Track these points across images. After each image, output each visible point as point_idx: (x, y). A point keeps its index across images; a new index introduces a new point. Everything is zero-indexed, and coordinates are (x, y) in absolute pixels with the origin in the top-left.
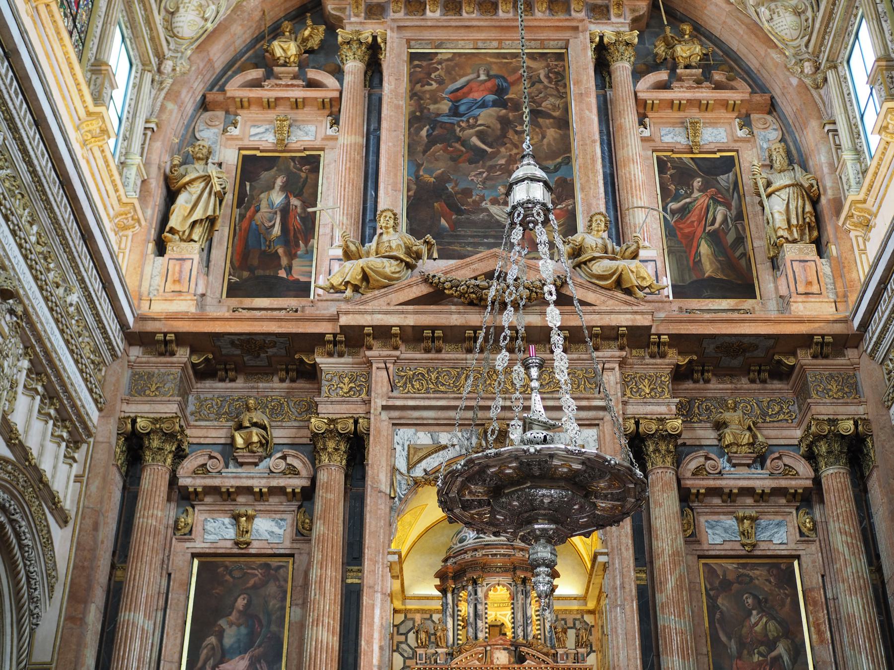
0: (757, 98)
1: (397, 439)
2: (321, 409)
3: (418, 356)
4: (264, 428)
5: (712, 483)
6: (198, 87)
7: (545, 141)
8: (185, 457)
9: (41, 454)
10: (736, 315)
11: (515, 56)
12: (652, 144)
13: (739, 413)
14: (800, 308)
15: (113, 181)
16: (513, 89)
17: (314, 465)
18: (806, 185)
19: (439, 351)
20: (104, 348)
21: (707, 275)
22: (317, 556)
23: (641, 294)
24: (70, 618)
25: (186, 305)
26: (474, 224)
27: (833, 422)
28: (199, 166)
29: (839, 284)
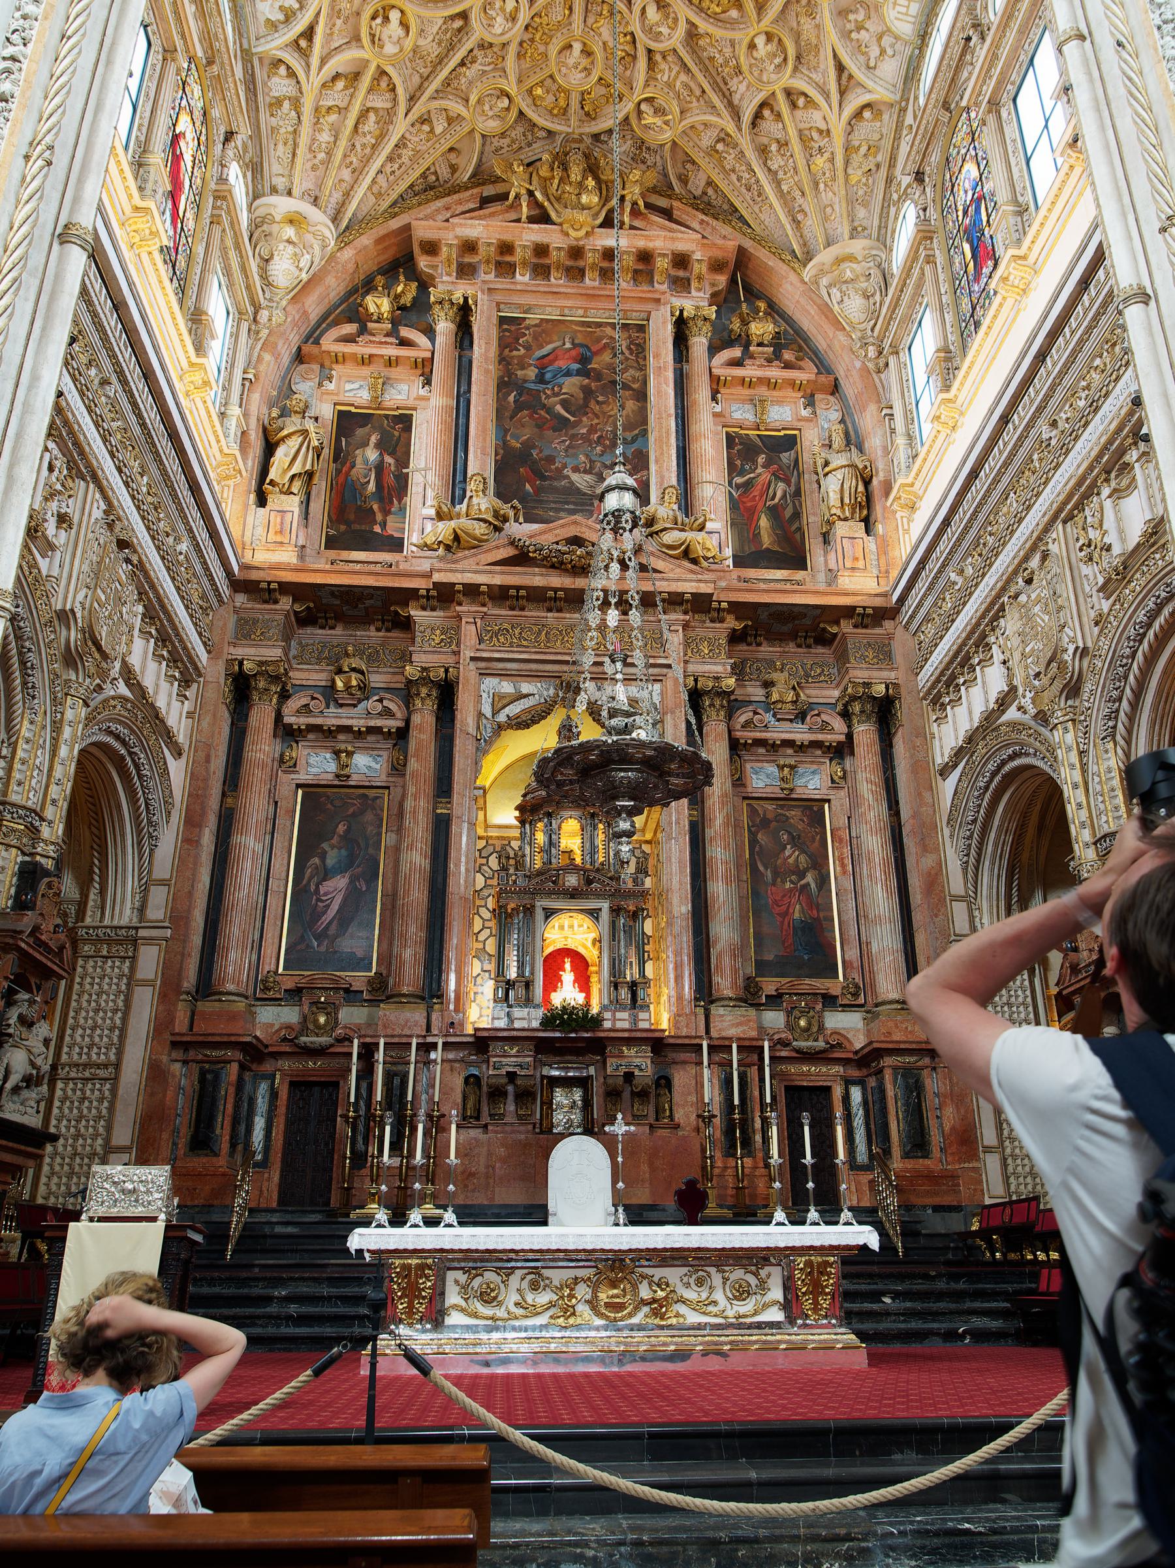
0: (823, 379)
1: (483, 687)
2: (415, 658)
3: (503, 612)
4: (362, 673)
5: (758, 735)
6: (294, 339)
8: (289, 697)
9: (156, 693)
10: (788, 586)
11: (599, 325)
13: (786, 674)
14: (846, 582)
15: (215, 432)
16: (596, 359)
17: (408, 708)
19: (522, 609)
20: (211, 595)
22: (411, 789)
23: (705, 564)
24: (186, 840)
25: (288, 556)
26: (556, 490)
27: (867, 685)
28: (296, 419)
29: (883, 561)
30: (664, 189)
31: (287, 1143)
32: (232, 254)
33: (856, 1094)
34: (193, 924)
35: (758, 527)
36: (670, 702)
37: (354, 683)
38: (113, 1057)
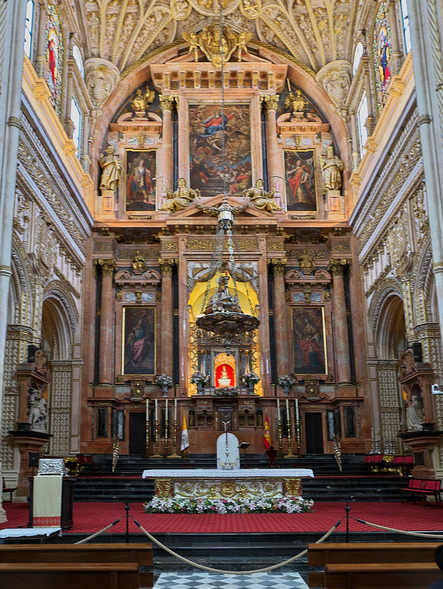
1: (189, 266)
4: (142, 261)
7: (241, 145)
11: (230, 106)
12: (283, 146)
18: (339, 166)
21: (300, 201)
22: (164, 307)
24: (85, 329)
25: (111, 217)
26: (214, 181)
28: (110, 157)
29: (347, 207)
30: (256, 40)
31: (130, 433)
32: (79, 89)
33: (331, 415)
34: (91, 359)
35: (297, 193)
36: (261, 270)
37: (140, 266)
38: (69, 406)
